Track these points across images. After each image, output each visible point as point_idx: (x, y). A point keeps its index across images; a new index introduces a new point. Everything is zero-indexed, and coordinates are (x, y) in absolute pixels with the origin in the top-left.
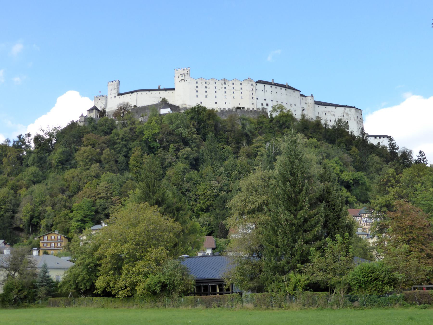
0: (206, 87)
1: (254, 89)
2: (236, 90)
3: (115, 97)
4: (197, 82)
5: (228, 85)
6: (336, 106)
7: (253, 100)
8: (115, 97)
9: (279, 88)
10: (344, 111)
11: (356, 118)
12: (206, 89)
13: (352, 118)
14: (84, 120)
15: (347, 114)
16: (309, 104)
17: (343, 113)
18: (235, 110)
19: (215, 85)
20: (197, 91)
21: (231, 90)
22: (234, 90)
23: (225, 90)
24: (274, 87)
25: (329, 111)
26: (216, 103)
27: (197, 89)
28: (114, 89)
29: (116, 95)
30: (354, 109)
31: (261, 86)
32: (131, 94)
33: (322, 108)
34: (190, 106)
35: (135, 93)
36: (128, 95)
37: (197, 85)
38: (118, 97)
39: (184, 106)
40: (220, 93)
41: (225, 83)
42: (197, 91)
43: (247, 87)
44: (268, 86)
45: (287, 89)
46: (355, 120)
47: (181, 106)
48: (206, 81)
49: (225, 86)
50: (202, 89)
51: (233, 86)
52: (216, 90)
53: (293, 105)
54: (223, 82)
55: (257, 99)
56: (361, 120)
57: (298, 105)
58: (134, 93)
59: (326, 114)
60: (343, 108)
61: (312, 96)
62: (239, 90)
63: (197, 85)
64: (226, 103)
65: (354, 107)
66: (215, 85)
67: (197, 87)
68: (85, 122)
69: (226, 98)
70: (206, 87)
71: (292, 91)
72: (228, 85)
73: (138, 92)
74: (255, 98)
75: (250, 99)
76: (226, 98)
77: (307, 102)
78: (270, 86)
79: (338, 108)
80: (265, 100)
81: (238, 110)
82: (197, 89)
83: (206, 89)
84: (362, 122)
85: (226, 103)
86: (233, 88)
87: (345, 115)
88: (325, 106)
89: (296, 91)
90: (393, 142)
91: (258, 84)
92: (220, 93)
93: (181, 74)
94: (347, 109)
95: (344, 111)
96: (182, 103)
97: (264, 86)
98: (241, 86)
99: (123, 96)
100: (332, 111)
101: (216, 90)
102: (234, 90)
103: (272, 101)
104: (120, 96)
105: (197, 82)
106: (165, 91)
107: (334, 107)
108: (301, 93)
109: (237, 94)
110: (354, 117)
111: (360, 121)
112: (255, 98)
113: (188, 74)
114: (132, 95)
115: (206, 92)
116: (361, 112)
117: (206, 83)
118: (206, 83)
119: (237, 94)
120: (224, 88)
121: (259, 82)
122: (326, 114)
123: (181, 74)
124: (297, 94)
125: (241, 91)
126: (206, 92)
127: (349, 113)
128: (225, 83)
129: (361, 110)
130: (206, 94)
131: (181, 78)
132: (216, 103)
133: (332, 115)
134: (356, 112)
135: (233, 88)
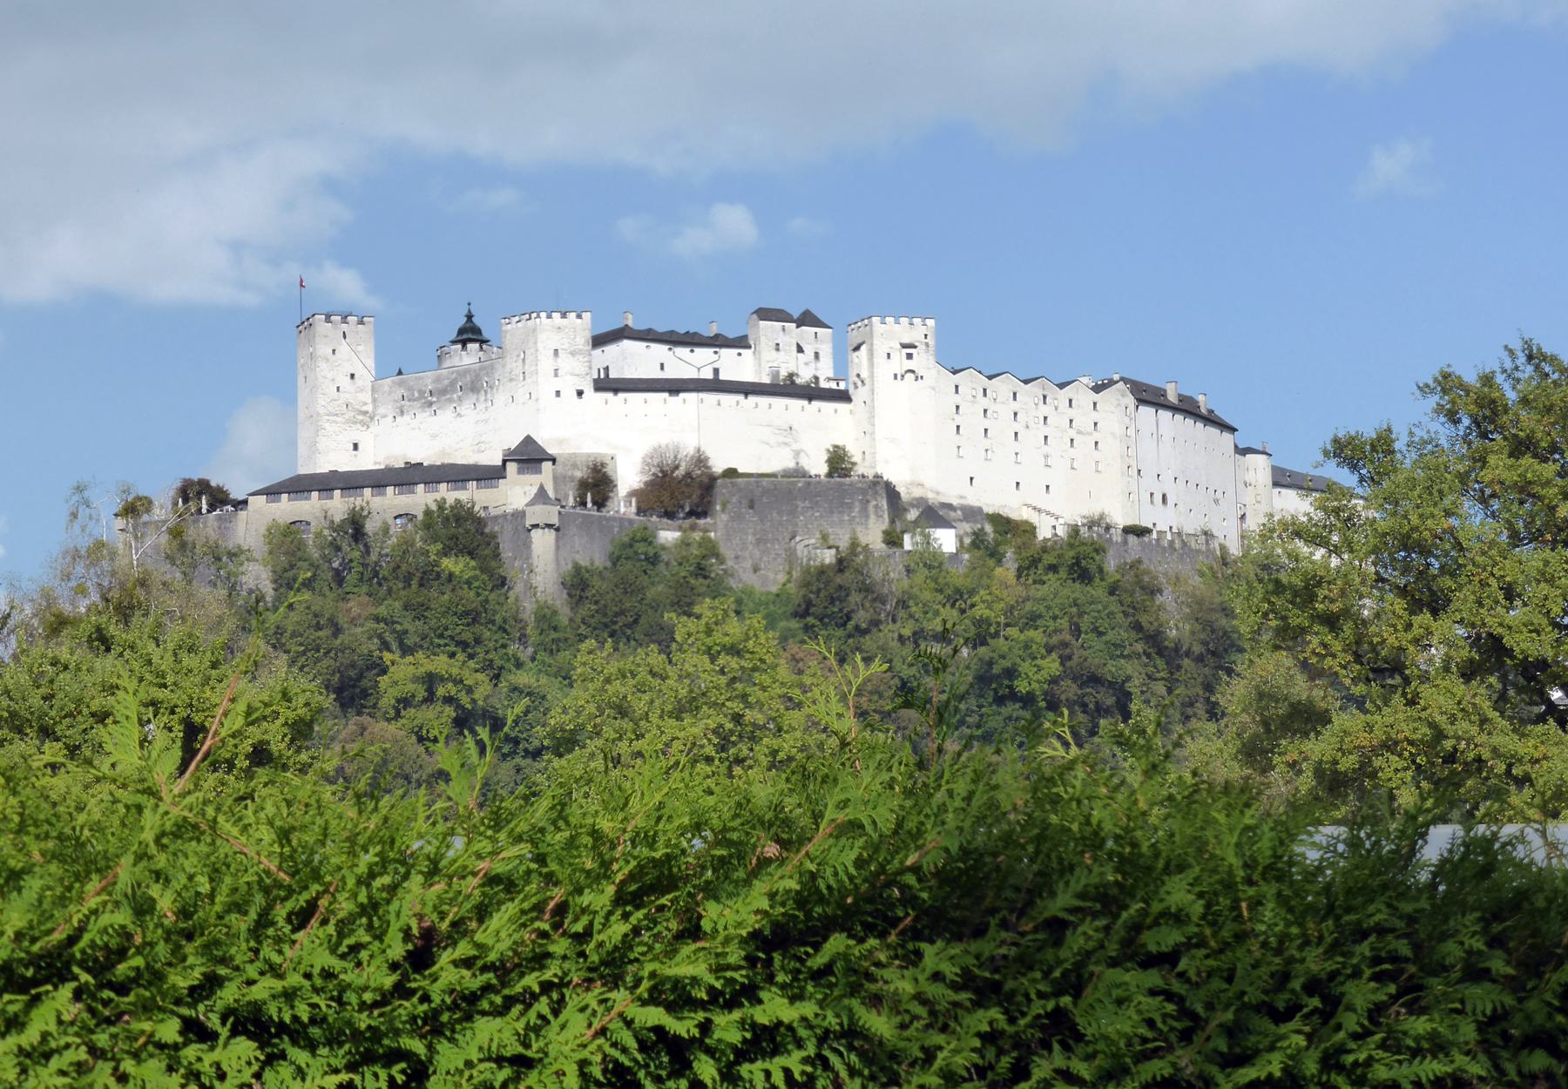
2: (1079, 432)
3: (580, 393)
8: (580, 393)
12: (986, 423)
18: (1119, 540)
19: (1015, 406)
22: (1072, 433)
27: (959, 420)
28: (573, 354)
32: (666, 395)
34: (938, 493)
35: (691, 397)
36: (658, 400)
49: (1045, 410)
51: (1071, 413)
58: (682, 395)
62: (1090, 434)
68: (558, 530)
81: (1132, 539)
82: (959, 420)
83: (986, 423)
93: (904, 346)
98: (1095, 416)
99: (622, 395)
101: (1018, 427)
102: (1072, 433)
104: (609, 395)
123: (904, 346)
128: (1045, 397)
130: (986, 443)
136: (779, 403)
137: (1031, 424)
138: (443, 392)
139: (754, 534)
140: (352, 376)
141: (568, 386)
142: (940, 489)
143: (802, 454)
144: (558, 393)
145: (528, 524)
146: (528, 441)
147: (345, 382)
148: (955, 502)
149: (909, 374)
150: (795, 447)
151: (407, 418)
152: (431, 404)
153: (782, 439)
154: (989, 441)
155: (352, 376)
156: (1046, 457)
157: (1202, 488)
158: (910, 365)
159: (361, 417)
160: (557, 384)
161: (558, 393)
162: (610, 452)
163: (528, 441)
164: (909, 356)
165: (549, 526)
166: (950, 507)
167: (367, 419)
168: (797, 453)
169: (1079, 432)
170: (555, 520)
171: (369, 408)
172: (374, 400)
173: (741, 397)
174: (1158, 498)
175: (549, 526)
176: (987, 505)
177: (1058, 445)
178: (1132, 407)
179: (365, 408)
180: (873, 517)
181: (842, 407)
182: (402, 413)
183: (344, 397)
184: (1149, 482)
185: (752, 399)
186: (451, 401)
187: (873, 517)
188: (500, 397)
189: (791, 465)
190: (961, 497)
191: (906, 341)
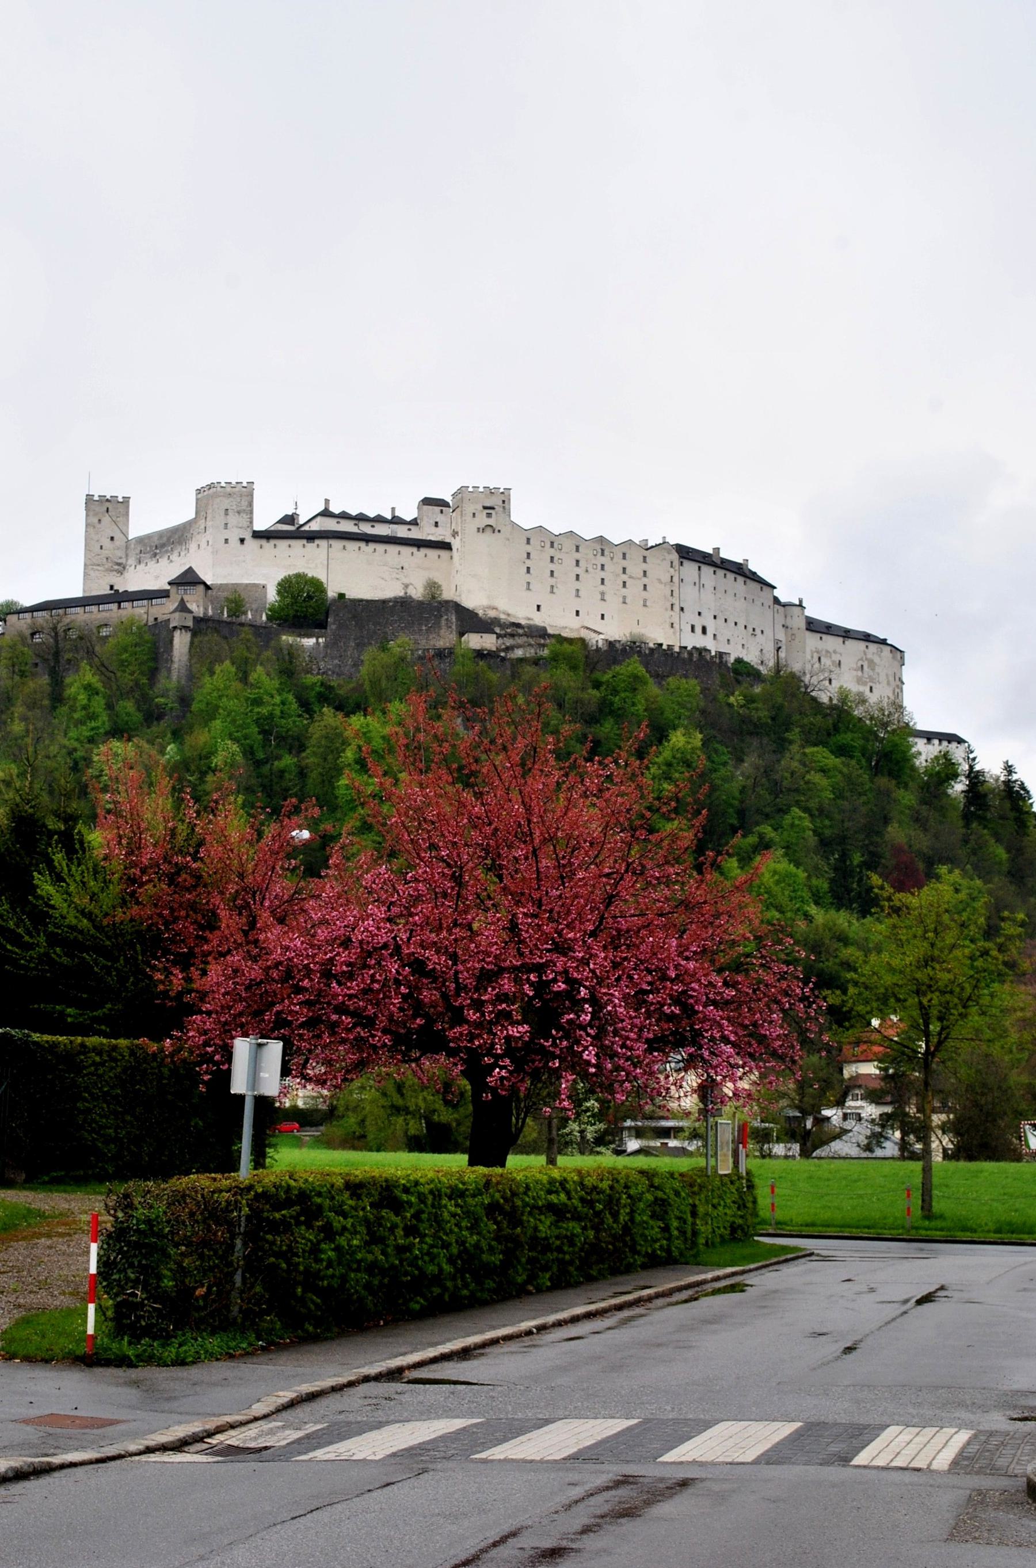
0: (552, 558)
1: (676, 579)
2: (631, 577)
3: (242, 541)
4: (528, 541)
5: (612, 559)
6: (846, 634)
7: (672, 613)
8: (242, 541)
9: (731, 576)
10: (865, 654)
11: (891, 679)
13: (883, 678)
14: (190, 624)
15: (872, 664)
16: (795, 631)
17: (861, 659)
19: (577, 556)
20: (528, 568)
21: (618, 575)
22: (625, 577)
23: (603, 574)
24: (721, 573)
25: (827, 652)
26: (577, 613)
28: (239, 512)
29: (248, 536)
30: (889, 648)
31: (690, 569)
32: (304, 541)
33: (812, 641)
34: (509, 615)
35: (323, 543)
37: (529, 549)
38: (252, 544)
39: (492, 614)
40: (590, 584)
41: (603, 551)
42: (528, 568)
43: (661, 568)
44: (707, 570)
45: (748, 581)
46: (888, 684)
47: (481, 613)
48: (553, 538)
49: (602, 560)
51: (624, 563)
52: (578, 571)
53: (758, 632)
54: (598, 547)
55: (682, 609)
56: (899, 683)
57: (769, 632)
58: (317, 542)
59: (819, 659)
60: (862, 645)
61: (800, 605)
63: (529, 549)
64: (603, 616)
65: (884, 642)
66: (577, 556)
67: (528, 554)
70: (552, 558)
71: (758, 586)
72: (612, 559)
73: (332, 542)
74: (677, 608)
75: (666, 610)
77: (789, 623)
78: (711, 569)
79: (850, 643)
80: (700, 614)
82: (529, 563)
83: (552, 567)
84: (902, 691)
85: (603, 616)
86: (624, 569)
87: (865, 667)
88: (819, 635)
89: (765, 587)
90: (1015, 777)
91: (685, 562)
92: (590, 584)
93: (485, 508)
94: (873, 647)
95: (865, 654)
96: (485, 602)
97: (699, 568)
98: (644, 566)
99: (273, 542)
100: (835, 652)
101: (578, 571)
103: (715, 617)
104: (264, 542)
105: (528, 541)
106: (414, 550)
107: (841, 639)
108: (776, 593)
109: (634, 589)
110: (887, 675)
111: (898, 686)
112: (677, 608)
113: (504, 508)
114: (311, 546)
115: (552, 572)
116: (902, 658)
117: (552, 544)
118: (552, 544)
119: (634, 589)
120: (599, 567)
121: (685, 553)
122: (819, 659)
123: (485, 508)
124: (766, 595)
125: (645, 580)
126: (552, 572)
127: (877, 659)
128: (603, 551)
129: (901, 651)
130: (552, 581)
131: (482, 520)
132: (577, 613)
134: (894, 658)
135: (624, 569)
136: (393, 549)
137: (590, 569)
138: (163, 545)
139: (355, 639)
140: (112, 538)
141: (234, 536)
142: (510, 612)
143: (411, 587)
144: (226, 541)
145: (171, 626)
146: (190, 570)
147: (106, 542)
148: (523, 622)
149: (489, 529)
150: (406, 581)
151: (142, 565)
152: (155, 555)
153: (395, 575)
154: (554, 580)
155: (112, 538)
156: (603, 594)
157: (741, 626)
158: (490, 522)
159: (116, 567)
160: (227, 534)
161: (226, 541)
162: (262, 582)
163: (190, 570)
164: (489, 515)
165: (186, 628)
166: (518, 625)
167: (120, 568)
168: (406, 586)
169: (631, 577)
170: (190, 624)
171: (123, 561)
172: (127, 555)
173: (362, 545)
175: (186, 628)
176: (552, 626)
177: (612, 588)
178: (676, 563)
179: (120, 561)
180: (444, 628)
181: (444, 553)
182: (140, 562)
183: (105, 553)
184: (690, 617)
185: (372, 546)
186: (167, 551)
187: (444, 628)
188: (193, 546)
189: (402, 594)
190: (529, 619)
191: (488, 505)
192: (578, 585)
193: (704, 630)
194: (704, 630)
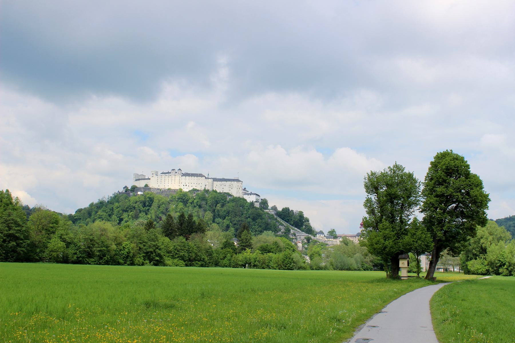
13: (235, 186)
15: (232, 185)
37: (158, 178)
39: (153, 188)
49: (168, 178)
50: (159, 180)
52: (165, 180)
63: (158, 178)
69: (168, 183)
74: (180, 183)
76: (168, 183)
82: (158, 180)
101: (165, 180)
109: (173, 182)
112: (180, 183)
119: (173, 182)
127: (233, 184)
130: (161, 182)
133: (224, 185)
166: (156, 189)
174: (185, 185)
192: (165, 182)
193: (186, 185)
194: (186, 185)
